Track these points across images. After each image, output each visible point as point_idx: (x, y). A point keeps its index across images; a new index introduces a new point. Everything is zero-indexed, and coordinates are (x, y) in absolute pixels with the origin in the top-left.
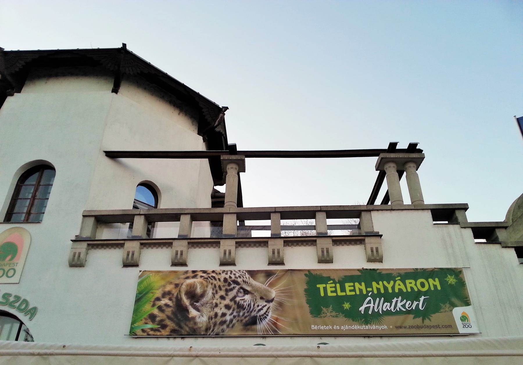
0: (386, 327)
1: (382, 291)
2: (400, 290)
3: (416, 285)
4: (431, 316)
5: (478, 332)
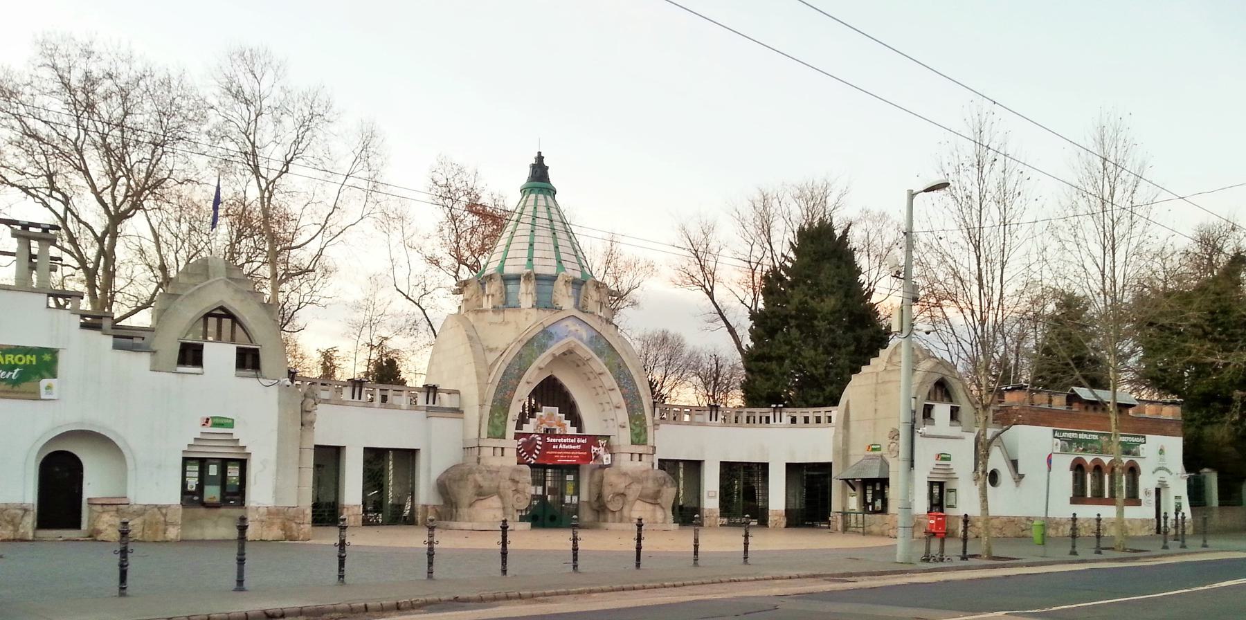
3: (14, 359)
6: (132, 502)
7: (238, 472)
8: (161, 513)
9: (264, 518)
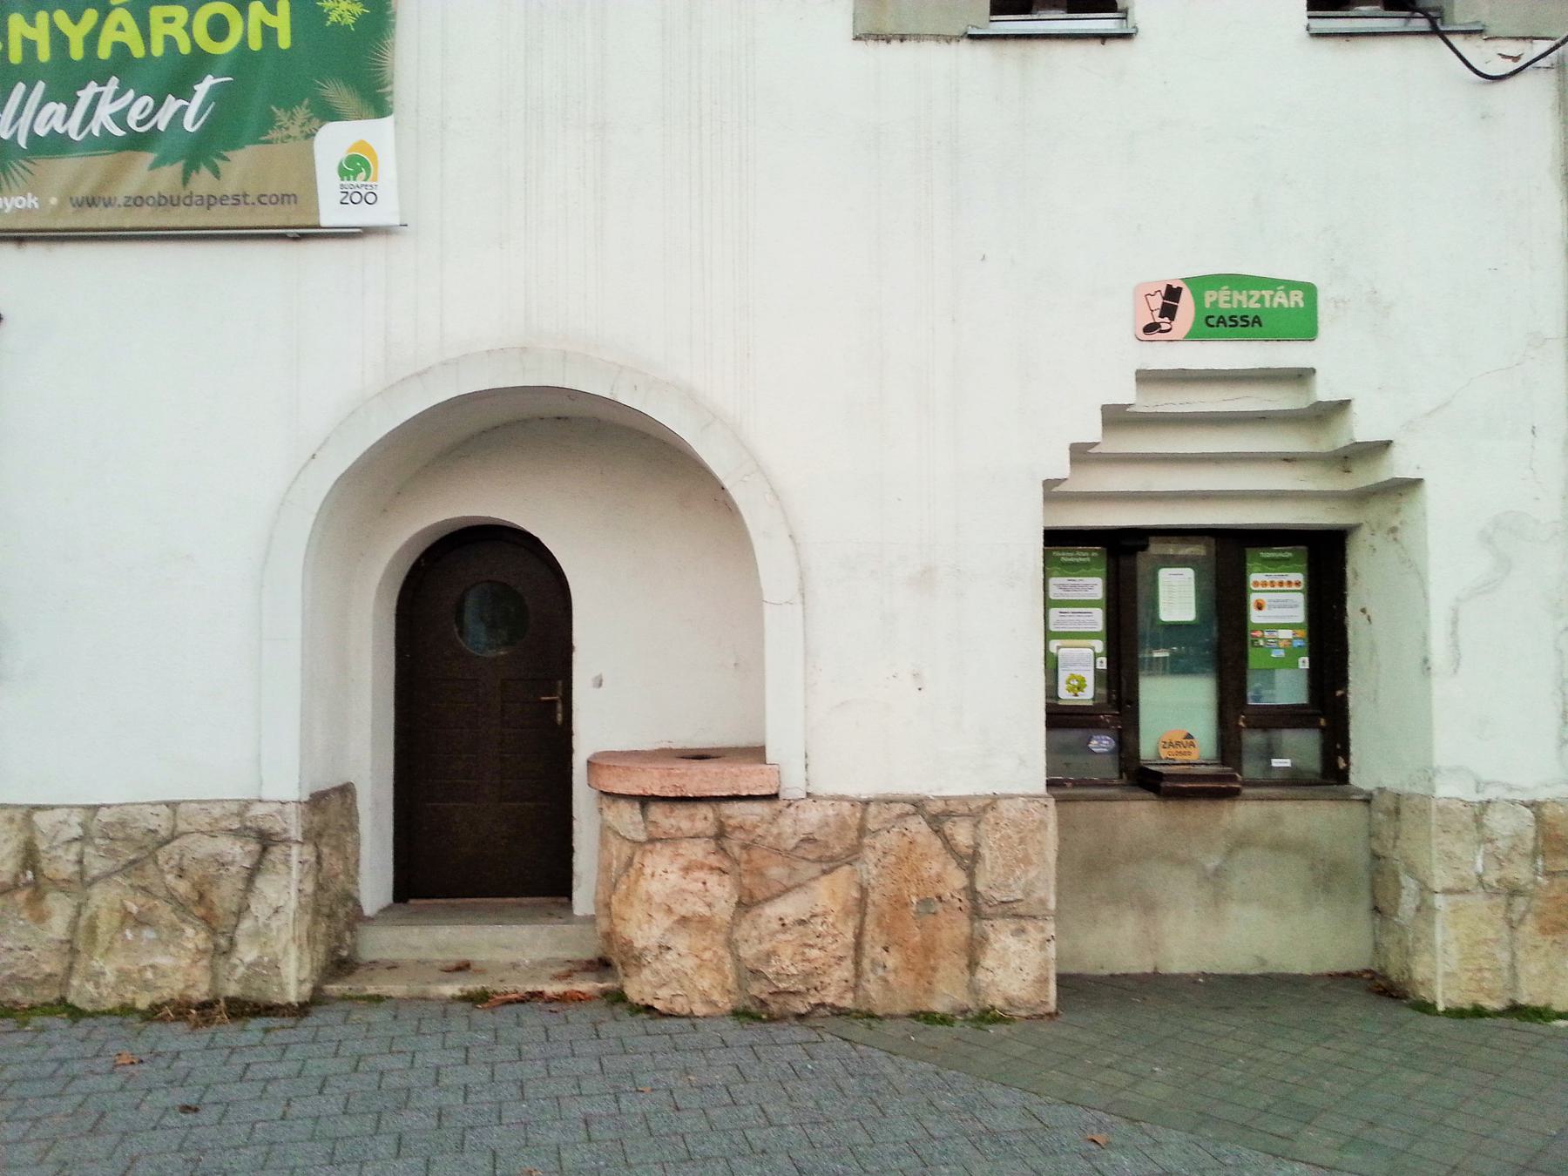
0: (31, 201)
1: (44, 54)
2: (121, 49)
3: (188, 28)
4: (225, 159)
5: (395, 221)
6: (793, 786)
7: (1300, 599)
8: (947, 842)
9: (1521, 872)
